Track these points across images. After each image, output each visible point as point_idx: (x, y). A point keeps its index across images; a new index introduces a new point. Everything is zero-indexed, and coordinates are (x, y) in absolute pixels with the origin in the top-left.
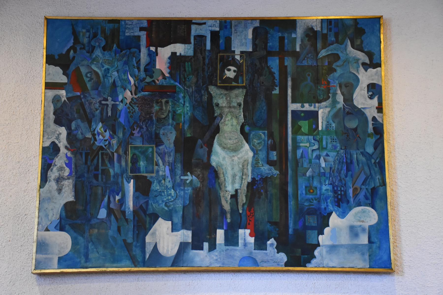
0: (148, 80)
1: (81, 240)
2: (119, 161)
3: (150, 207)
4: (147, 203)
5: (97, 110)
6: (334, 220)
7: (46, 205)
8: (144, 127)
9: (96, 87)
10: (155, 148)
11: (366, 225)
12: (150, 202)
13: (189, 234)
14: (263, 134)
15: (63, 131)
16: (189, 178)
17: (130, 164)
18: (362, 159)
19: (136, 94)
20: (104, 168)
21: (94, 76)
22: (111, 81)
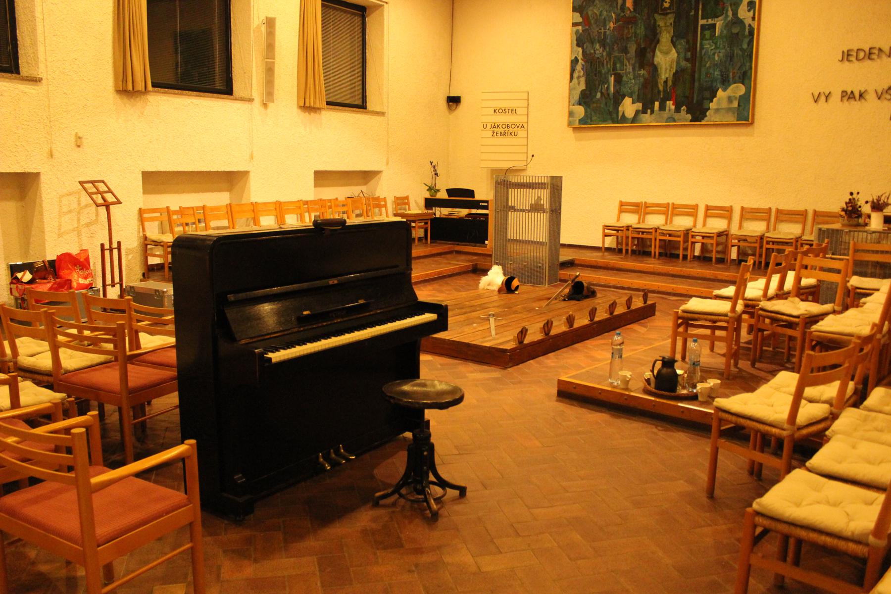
0: (622, 14)
6: (720, 93)
11: (737, 96)
14: (683, 42)
15: (580, 50)
16: (642, 72)
18: (740, 53)
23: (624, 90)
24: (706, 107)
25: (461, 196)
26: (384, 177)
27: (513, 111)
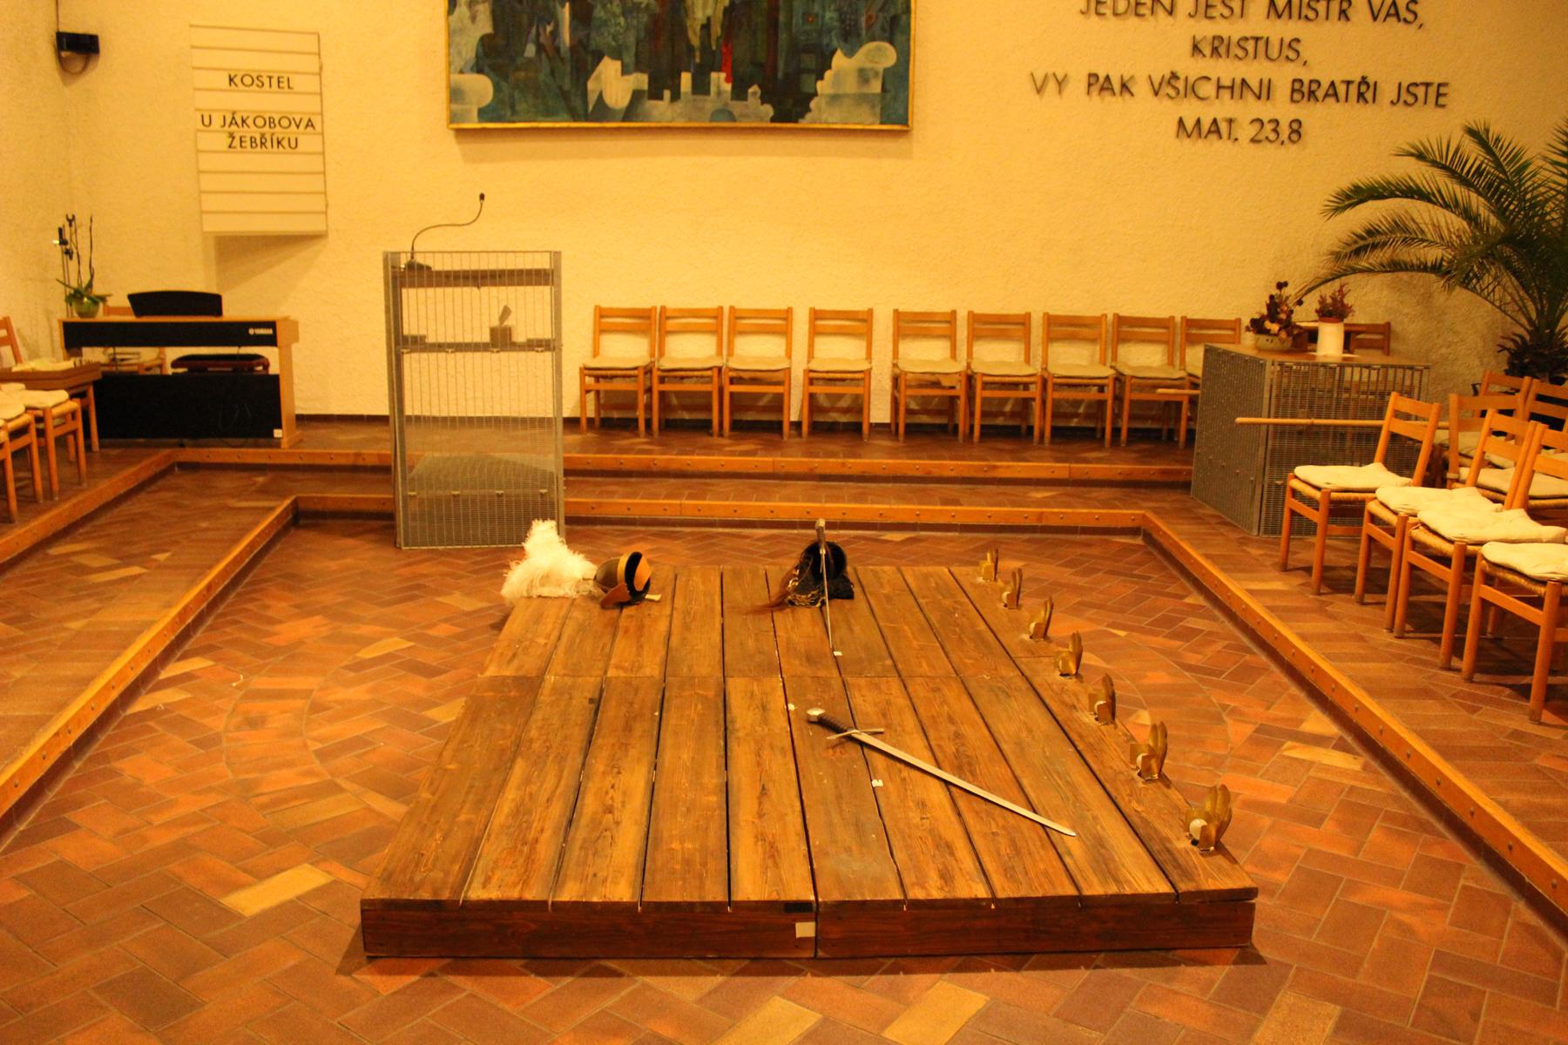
1: (504, 85)
6: (839, 60)
7: (457, 39)
11: (880, 68)
12: (593, 34)
24: (807, 89)
25: (172, 312)
27: (281, 82)
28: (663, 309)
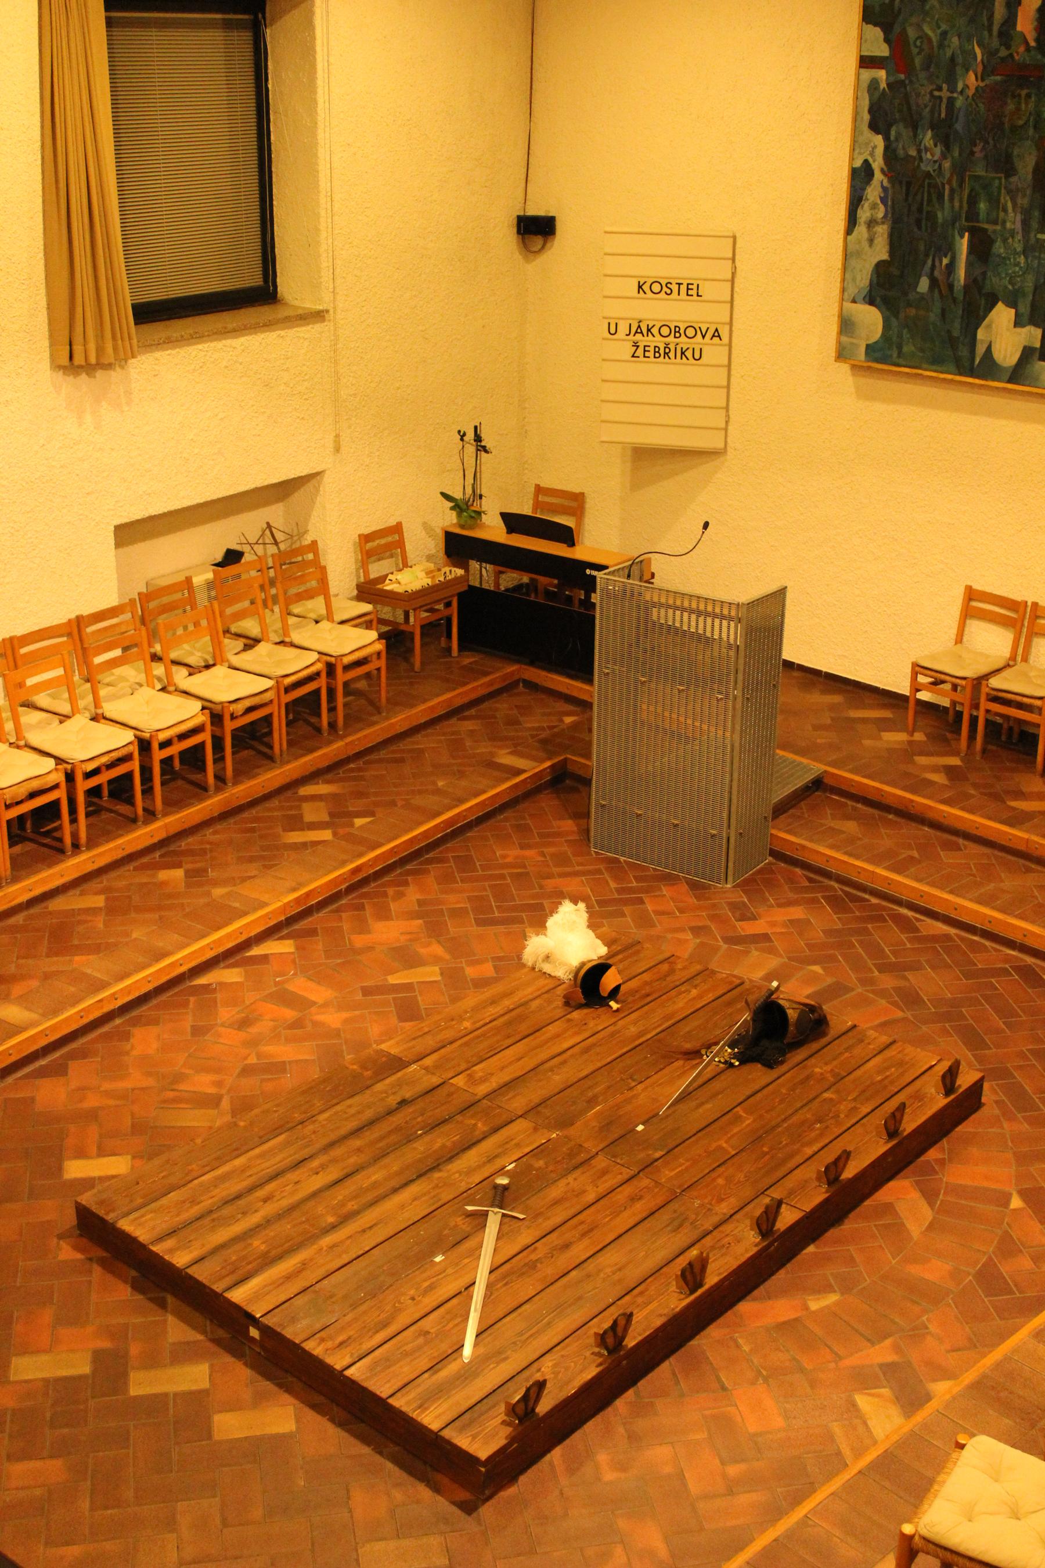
0: (1003, 53)
1: (894, 322)
2: (952, 199)
3: (988, 282)
4: (984, 274)
5: (926, 106)
8: (991, 142)
9: (926, 67)
10: (1003, 180)
12: (989, 274)
13: (1038, 333)
15: (879, 141)
17: (965, 206)
19: (983, 80)
20: (929, 209)
21: (925, 47)
22: (949, 54)
23: (997, 282)
26: (328, 483)
27: (691, 290)
28: (1035, 605)
